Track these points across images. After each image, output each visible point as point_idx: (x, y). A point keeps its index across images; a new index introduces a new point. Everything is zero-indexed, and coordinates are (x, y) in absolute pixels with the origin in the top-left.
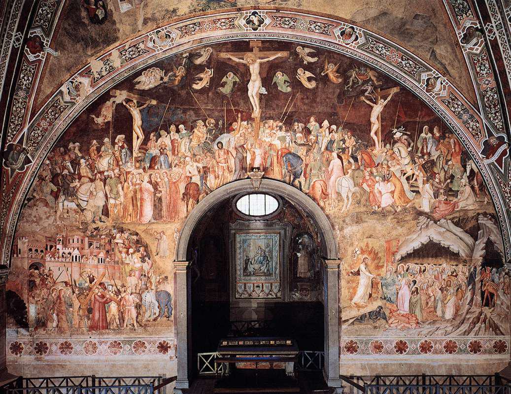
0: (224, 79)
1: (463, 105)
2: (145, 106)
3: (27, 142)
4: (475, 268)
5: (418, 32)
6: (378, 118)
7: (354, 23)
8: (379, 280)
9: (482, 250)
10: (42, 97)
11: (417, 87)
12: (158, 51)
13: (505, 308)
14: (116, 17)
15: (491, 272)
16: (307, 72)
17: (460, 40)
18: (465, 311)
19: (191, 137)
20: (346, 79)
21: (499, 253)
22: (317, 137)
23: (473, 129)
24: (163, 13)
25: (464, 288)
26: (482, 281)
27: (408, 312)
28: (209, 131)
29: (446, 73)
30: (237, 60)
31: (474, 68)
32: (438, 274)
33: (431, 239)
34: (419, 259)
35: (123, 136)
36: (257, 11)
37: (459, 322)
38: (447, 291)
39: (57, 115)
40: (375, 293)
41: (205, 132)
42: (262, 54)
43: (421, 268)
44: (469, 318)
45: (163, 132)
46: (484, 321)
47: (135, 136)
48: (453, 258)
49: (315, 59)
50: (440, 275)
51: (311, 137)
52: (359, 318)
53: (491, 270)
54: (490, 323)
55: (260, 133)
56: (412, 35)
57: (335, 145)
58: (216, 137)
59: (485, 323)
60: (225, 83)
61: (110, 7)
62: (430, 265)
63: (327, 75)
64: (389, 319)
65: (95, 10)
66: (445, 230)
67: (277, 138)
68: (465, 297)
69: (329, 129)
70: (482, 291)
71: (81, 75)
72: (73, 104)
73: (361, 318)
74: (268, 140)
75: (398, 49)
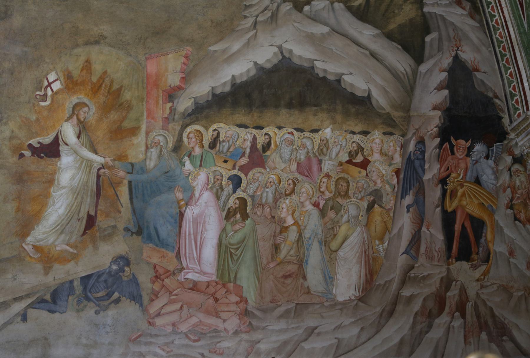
4: (421, 142)
8: (122, 174)
9: (439, 88)
13: (523, 267)
15: (468, 155)
18: (396, 275)
21: (492, 99)
25: (389, 201)
26: (443, 182)
27: (214, 278)
32: (308, 158)
33: (287, 55)
34: (252, 110)
37: (379, 309)
38: (337, 209)
40: (107, 215)
43: (255, 139)
44: (410, 299)
46: (461, 308)
48: (353, 110)
50: (314, 161)
52: (48, 297)
53: (470, 149)
54: (478, 316)
59: (463, 316)
62: (284, 131)
64: (152, 300)
66: (325, 29)
68: (395, 231)
70: (444, 212)
73: (55, 295)
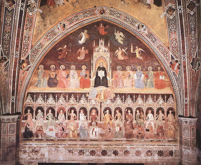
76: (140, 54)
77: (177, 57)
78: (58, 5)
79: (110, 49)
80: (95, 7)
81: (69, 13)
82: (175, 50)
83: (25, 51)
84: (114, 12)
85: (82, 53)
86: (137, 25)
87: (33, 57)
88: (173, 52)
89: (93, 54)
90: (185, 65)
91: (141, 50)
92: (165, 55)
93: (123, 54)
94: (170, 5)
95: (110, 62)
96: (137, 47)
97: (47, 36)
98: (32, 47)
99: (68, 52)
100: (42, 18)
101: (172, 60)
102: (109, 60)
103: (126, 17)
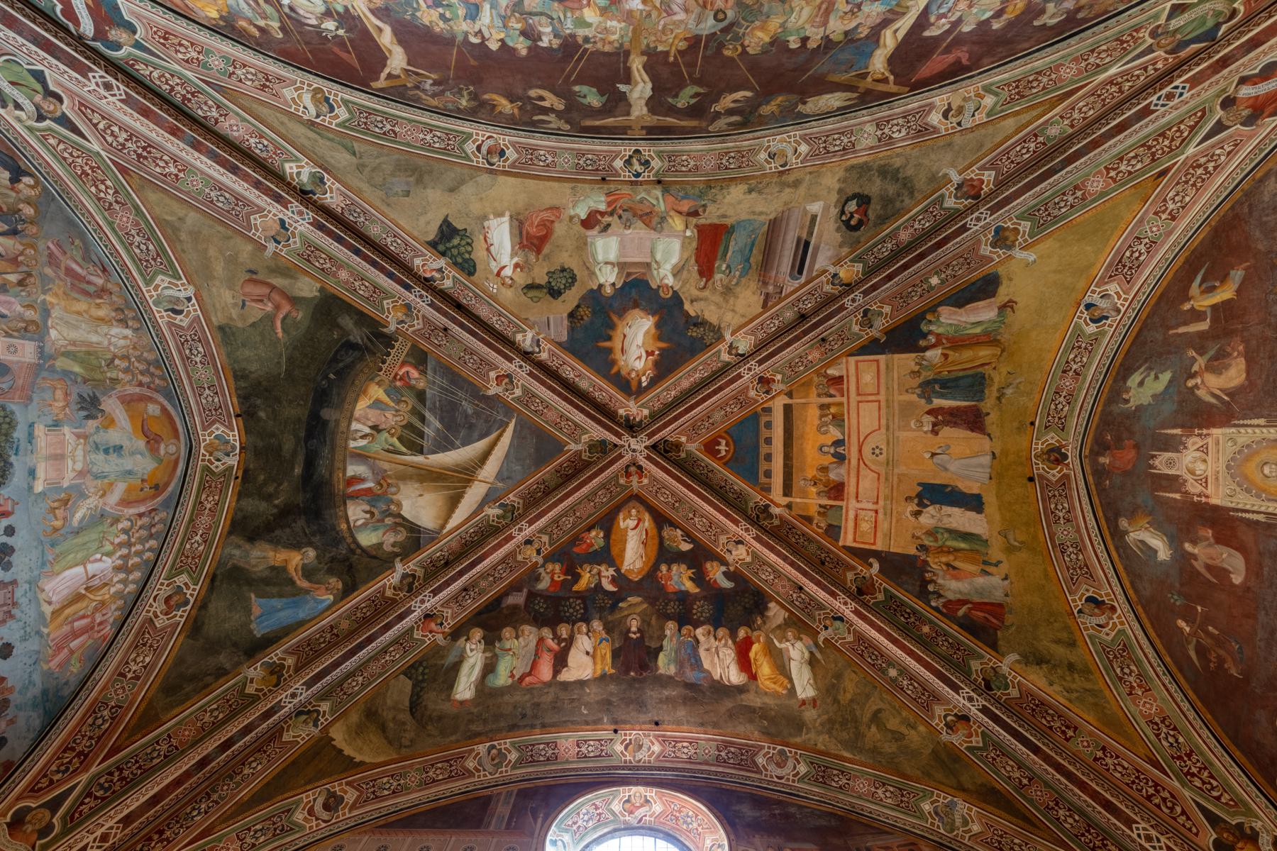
0: (693, 101)
1: (240, 81)
2: (854, 73)
3: (1135, 49)
5: (393, 175)
6: (390, 51)
7: (491, 172)
10: (1025, 118)
11: (338, 93)
12: (795, 136)
14: (834, 197)
16: (549, 106)
17: (326, 175)
19: (779, 30)
20: (474, 97)
22: (505, 26)
23: (180, 45)
24: (766, 191)
28: (737, 38)
29: (311, 124)
30: (668, 119)
31: (271, 141)
35: (927, 34)
36: (633, 179)
39: (1031, 78)
41: (746, 37)
42: (627, 123)
45: (837, 37)
47: (900, 35)
49: (536, 118)
51: (519, 26)
55: (630, 34)
56: (400, 170)
57: (461, 12)
58: (725, 30)
60: (692, 97)
61: (834, 211)
63: (511, 102)
65: (856, 212)
67: (594, 26)
69: (483, 37)
71: (936, 130)
72: (987, 89)
74: (611, 23)
75: (408, 145)
76: (1217, 284)
77: (1202, 117)
78: (1007, 595)
79: (1192, 427)
80: (1031, 479)
81: (1045, 570)
82: (1167, 143)
83: (1169, 804)
84: (1049, 414)
85: (1212, 558)
86: (1092, 329)
87: (1215, 794)
88: (1180, 144)
89: (1216, 508)
90: (1209, 67)
91: (1200, 286)
92: (1211, 169)
93: (1216, 363)
94: (986, 250)
95: (1258, 426)
96: (1187, 307)
97: (1120, 679)
98: (1156, 764)
99: (1207, 619)
100: (1037, 664)
101: (1227, 123)
102: (1250, 430)
103: (1064, 372)
